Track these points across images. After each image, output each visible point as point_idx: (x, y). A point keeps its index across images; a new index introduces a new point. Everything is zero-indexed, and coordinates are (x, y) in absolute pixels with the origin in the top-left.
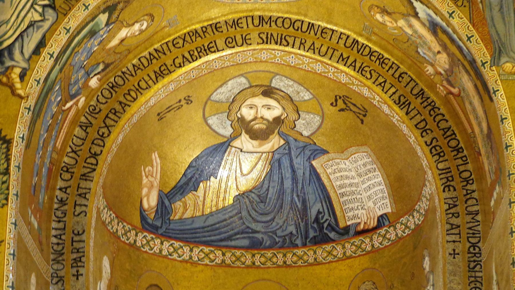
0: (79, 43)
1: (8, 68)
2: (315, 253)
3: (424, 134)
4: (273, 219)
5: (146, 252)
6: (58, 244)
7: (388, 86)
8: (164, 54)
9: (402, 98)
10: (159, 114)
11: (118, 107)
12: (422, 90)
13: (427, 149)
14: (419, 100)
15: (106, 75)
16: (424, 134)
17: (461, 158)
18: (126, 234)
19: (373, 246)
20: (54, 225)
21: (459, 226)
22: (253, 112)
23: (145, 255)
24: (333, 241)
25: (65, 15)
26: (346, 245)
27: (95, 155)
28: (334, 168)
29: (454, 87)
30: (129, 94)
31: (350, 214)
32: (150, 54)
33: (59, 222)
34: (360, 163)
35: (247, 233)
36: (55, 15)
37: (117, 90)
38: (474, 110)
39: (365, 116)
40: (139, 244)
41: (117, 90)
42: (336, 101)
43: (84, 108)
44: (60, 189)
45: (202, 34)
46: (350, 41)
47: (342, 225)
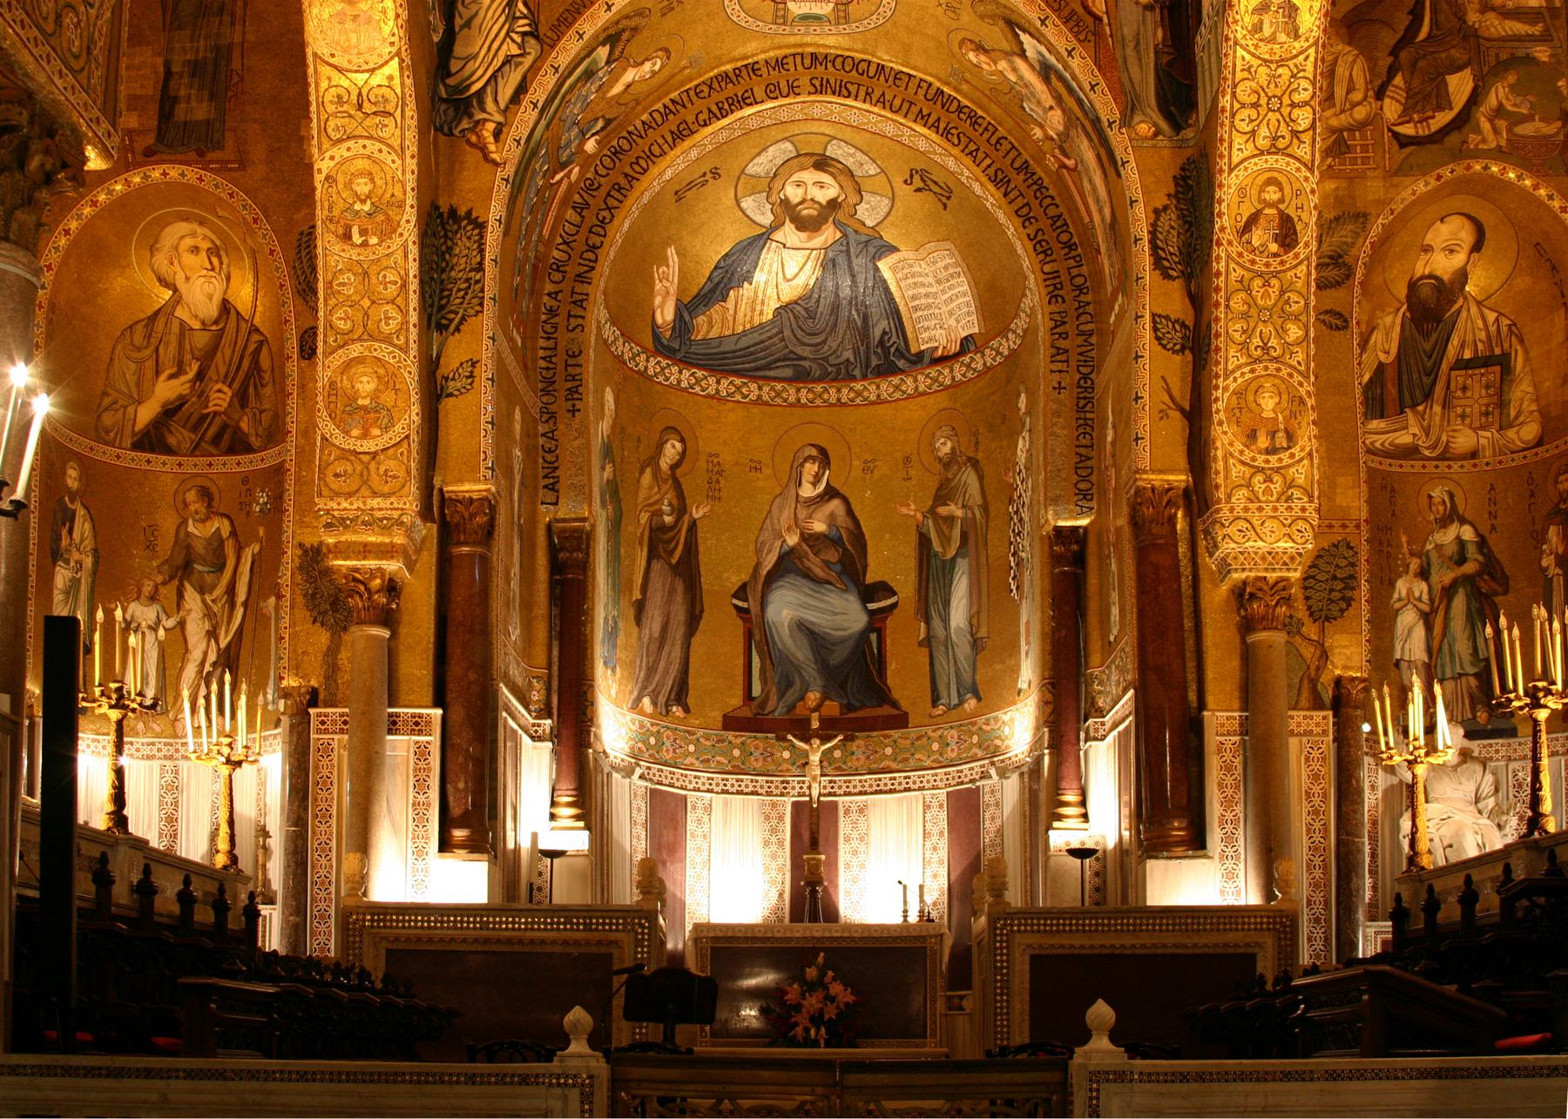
0: (571, 89)
1: (478, 122)
2: (878, 387)
3: (1027, 223)
4: (824, 342)
5: (660, 383)
6: (548, 369)
7: (981, 155)
8: (684, 106)
9: (999, 173)
10: (676, 193)
11: (623, 182)
12: (1026, 162)
13: (1030, 245)
14: (1022, 177)
15: (607, 136)
16: (1027, 223)
17: (1074, 258)
18: (633, 358)
19: (953, 378)
20: (542, 343)
21: (1067, 351)
22: (800, 191)
23: (659, 387)
24: (902, 371)
25: (552, 47)
26: (919, 377)
27: (594, 248)
28: (906, 271)
29: (1069, 158)
30: (638, 163)
31: (925, 335)
32: (665, 107)
33: (549, 339)
34: (940, 264)
35: (789, 359)
36: (539, 47)
37: (621, 157)
38: (1094, 189)
39: (948, 198)
40: (650, 371)
41: (621, 157)
42: (911, 176)
43: (578, 181)
44: (549, 294)
45: (734, 79)
46: (932, 92)
47: (914, 350)
